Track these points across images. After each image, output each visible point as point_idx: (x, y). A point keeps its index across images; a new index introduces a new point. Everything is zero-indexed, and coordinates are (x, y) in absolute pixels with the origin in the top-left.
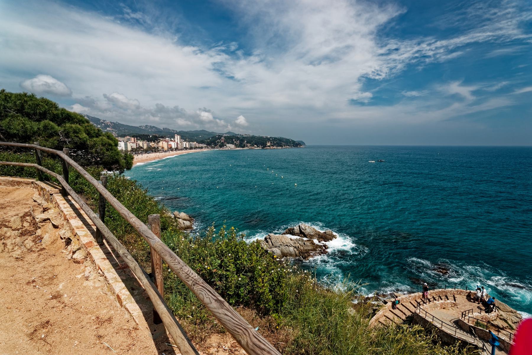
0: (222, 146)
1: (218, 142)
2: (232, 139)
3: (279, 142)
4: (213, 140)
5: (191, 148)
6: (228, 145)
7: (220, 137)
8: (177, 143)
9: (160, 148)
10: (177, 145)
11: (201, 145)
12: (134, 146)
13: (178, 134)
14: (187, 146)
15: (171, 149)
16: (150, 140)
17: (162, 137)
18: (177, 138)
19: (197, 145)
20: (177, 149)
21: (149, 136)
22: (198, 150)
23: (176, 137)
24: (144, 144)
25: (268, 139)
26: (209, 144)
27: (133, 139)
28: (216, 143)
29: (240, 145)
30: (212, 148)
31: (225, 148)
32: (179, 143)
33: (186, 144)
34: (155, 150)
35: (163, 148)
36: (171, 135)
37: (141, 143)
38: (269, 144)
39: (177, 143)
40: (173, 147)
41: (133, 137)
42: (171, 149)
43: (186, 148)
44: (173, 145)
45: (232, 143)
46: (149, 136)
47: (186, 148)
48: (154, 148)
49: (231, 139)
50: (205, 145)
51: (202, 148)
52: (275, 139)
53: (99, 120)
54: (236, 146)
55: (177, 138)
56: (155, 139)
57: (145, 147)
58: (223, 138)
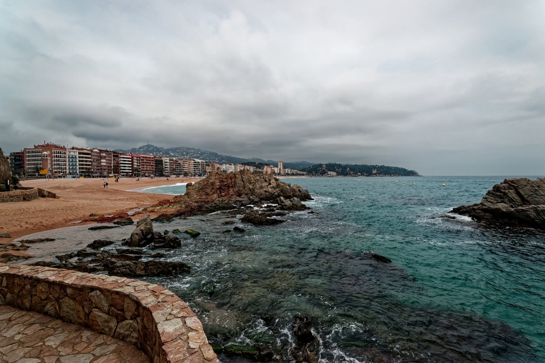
5: (293, 174)
6: (329, 173)
7: (321, 165)
8: (280, 169)
11: (301, 173)
14: (289, 172)
19: (299, 172)
28: (317, 171)
30: (313, 175)
32: (281, 168)
35: (267, 172)
39: (280, 169)
40: (276, 172)
43: (288, 174)
49: (332, 167)
51: (303, 175)
57: (252, 171)
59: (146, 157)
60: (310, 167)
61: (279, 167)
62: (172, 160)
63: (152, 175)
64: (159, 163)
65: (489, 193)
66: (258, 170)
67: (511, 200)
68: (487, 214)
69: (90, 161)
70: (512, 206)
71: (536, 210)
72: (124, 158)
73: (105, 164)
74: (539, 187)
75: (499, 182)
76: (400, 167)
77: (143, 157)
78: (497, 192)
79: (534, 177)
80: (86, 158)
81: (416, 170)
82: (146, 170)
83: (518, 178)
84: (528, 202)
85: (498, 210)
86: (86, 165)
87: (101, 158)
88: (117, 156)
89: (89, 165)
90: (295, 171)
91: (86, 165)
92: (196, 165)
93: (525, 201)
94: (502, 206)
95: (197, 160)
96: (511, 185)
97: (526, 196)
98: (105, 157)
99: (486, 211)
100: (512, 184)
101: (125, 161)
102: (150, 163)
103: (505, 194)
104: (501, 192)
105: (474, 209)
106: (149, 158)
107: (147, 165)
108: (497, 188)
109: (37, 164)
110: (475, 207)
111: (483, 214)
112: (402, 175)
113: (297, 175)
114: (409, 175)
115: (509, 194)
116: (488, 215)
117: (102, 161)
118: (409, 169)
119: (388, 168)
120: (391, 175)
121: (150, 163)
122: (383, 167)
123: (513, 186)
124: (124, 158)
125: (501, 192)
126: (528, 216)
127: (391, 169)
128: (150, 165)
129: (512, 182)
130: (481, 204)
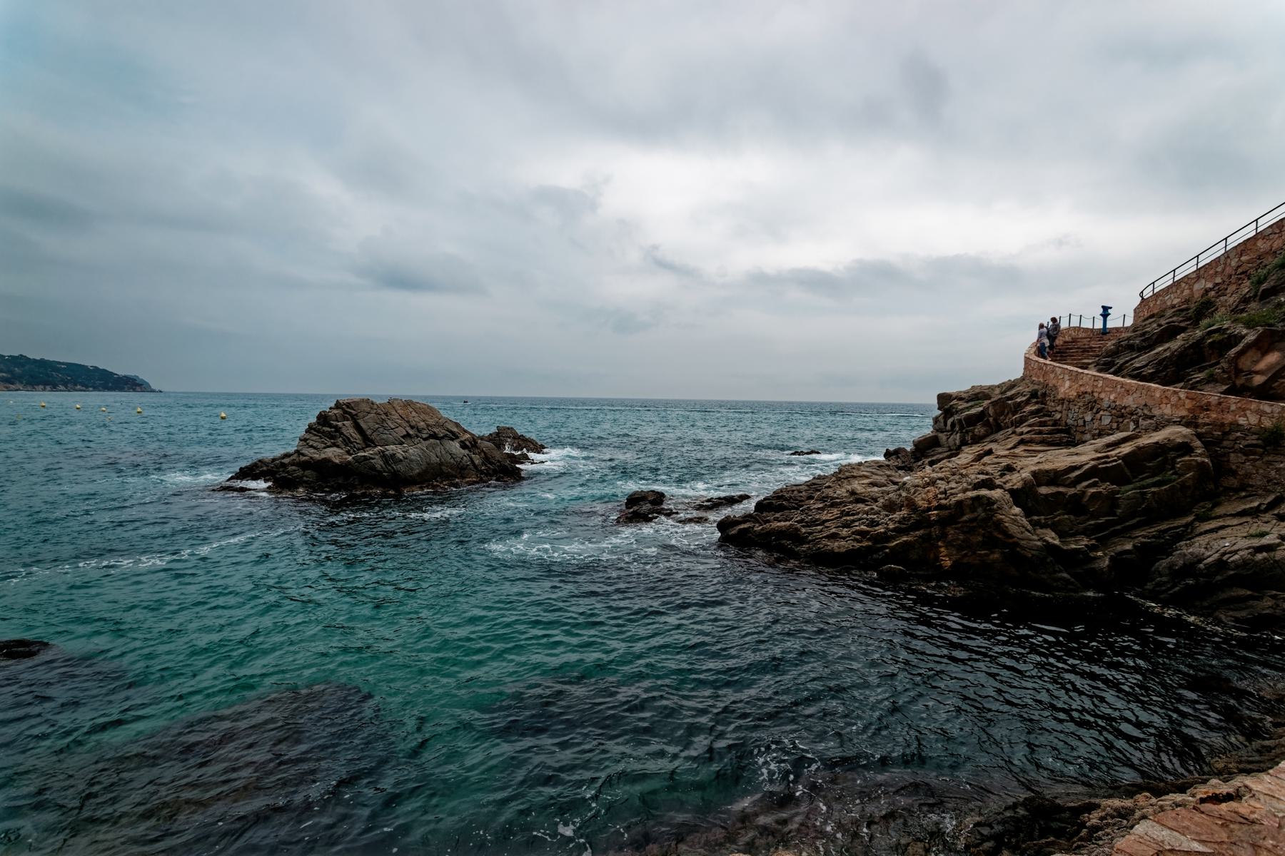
65: (310, 429)
67: (347, 441)
68: (307, 472)
70: (348, 453)
71: (383, 455)
74: (386, 414)
75: (326, 406)
76: (89, 362)
78: (324, 426)
79: (380, 397)
81: (143, 375)
83: (357, 399)
84: (372, 441)
85: (327, 460)
93: (368, 442)
94: (334, 454)
96: (346, 412)
97: (369, 432)
99: (305, 465)
100: (347, 409)
103: (338, 429)
104: (331, 426)
105: (283, 465)
108: (323, 418)
110: (286, 461)
111: (300, 473)
112: (96, 388)
114: (121, 389)
115: (344, 430)
116: (310, 475)
118: (120, 370)
119: (42, 363)
120: (54, 387)
122: (20, 360)
123: (350, 413)
125: (331, 426)
126: (373, 468)
127: (58, 370)
129: (348, 405)
130: (297, 452)
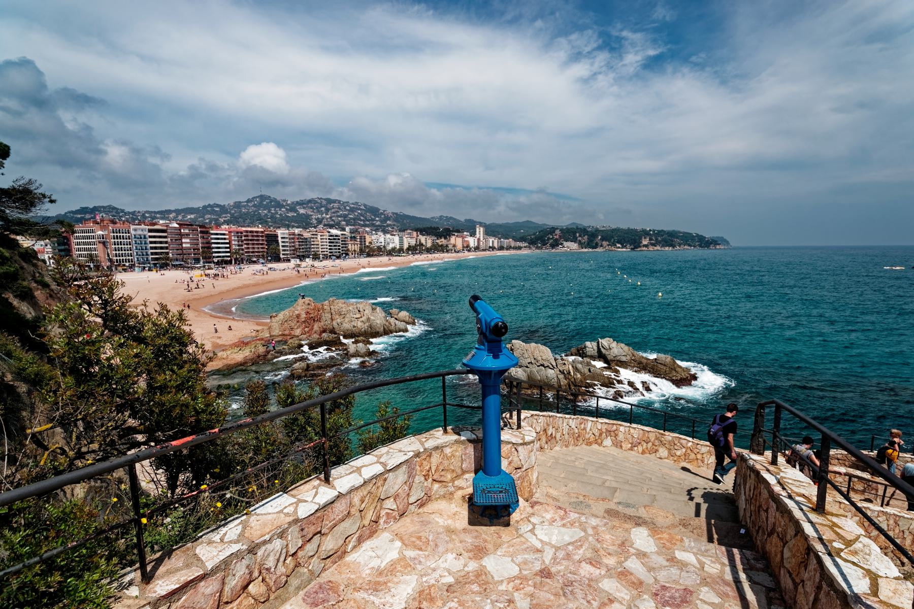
0: (555, 245)
1: (549, 239)
2: (575, 233)
3: (667, 238)
4: (542, 237)
5: (501, 248)
6: (566, 244)
7: (553, 230)
8: (479, 240)
9: (450, 247)
10: (478, 243)
11: (518, 244)
12: (413, 242)
13: (481, 224)
14: (496, 245)
15: (467, 248)
16: (439, 236)
17: (458, 231)
18: (480, 231)
19: (513, 244)
20: (477, 248)
21: (438, 228)
22: (513, 252)
23: (478, 230)
24: (427, 241)
25: (646, 233)
26: (532, 243)
27: (415, 233)
29: (588, 244)
30: (538, 248)
31: (560, 250)
33: (493, 241)
34: (443, 249)
35: (454, 246)
36: (470, 227)
37: (423, 239)
38: (645, 242)
39: (479, 240)
41: (416, 230)
42: (467, 248)
43: (493, 248)
44: (472, 242)
45: (574, 240)
46: (438, 228)
47: (493, 248)
48: (442, 245)
49: (570, 233)
50: (526, 244)
51: (520, 248)
52: (660, 233)
53: (378, 210)
54: (581, 245)
55: (480, 231)
56: (447, 233)
57: (429, 245)
58: (558, 232)
59: (251, 232)
60: (534, 234)
61: (478, 236)
62: (294, 234)
63: (261, 261)
64: (272, 239)
66: (442, 241)
69: (166, 242)
72: (217, 234)
73: (188, 245)
77: (247, 232)
80: (160, 237)
82: (253, 252)
86: (162, 248)
87: (182, 236)
88: (207, 232)
89: (167, 248)
90: (506, 242)
91: (162, 248)
92: (333, 239)
95: (334, 232)
98: (188, 235)
101: (218, 239)
102: (258, 240)
106: (257, 232)
107: (253, 244)
109: (90, 250)
113: (509, 248)
117: (184, 240)
121: (258, 240)
124: (217, 234)
128: (258, 244)
